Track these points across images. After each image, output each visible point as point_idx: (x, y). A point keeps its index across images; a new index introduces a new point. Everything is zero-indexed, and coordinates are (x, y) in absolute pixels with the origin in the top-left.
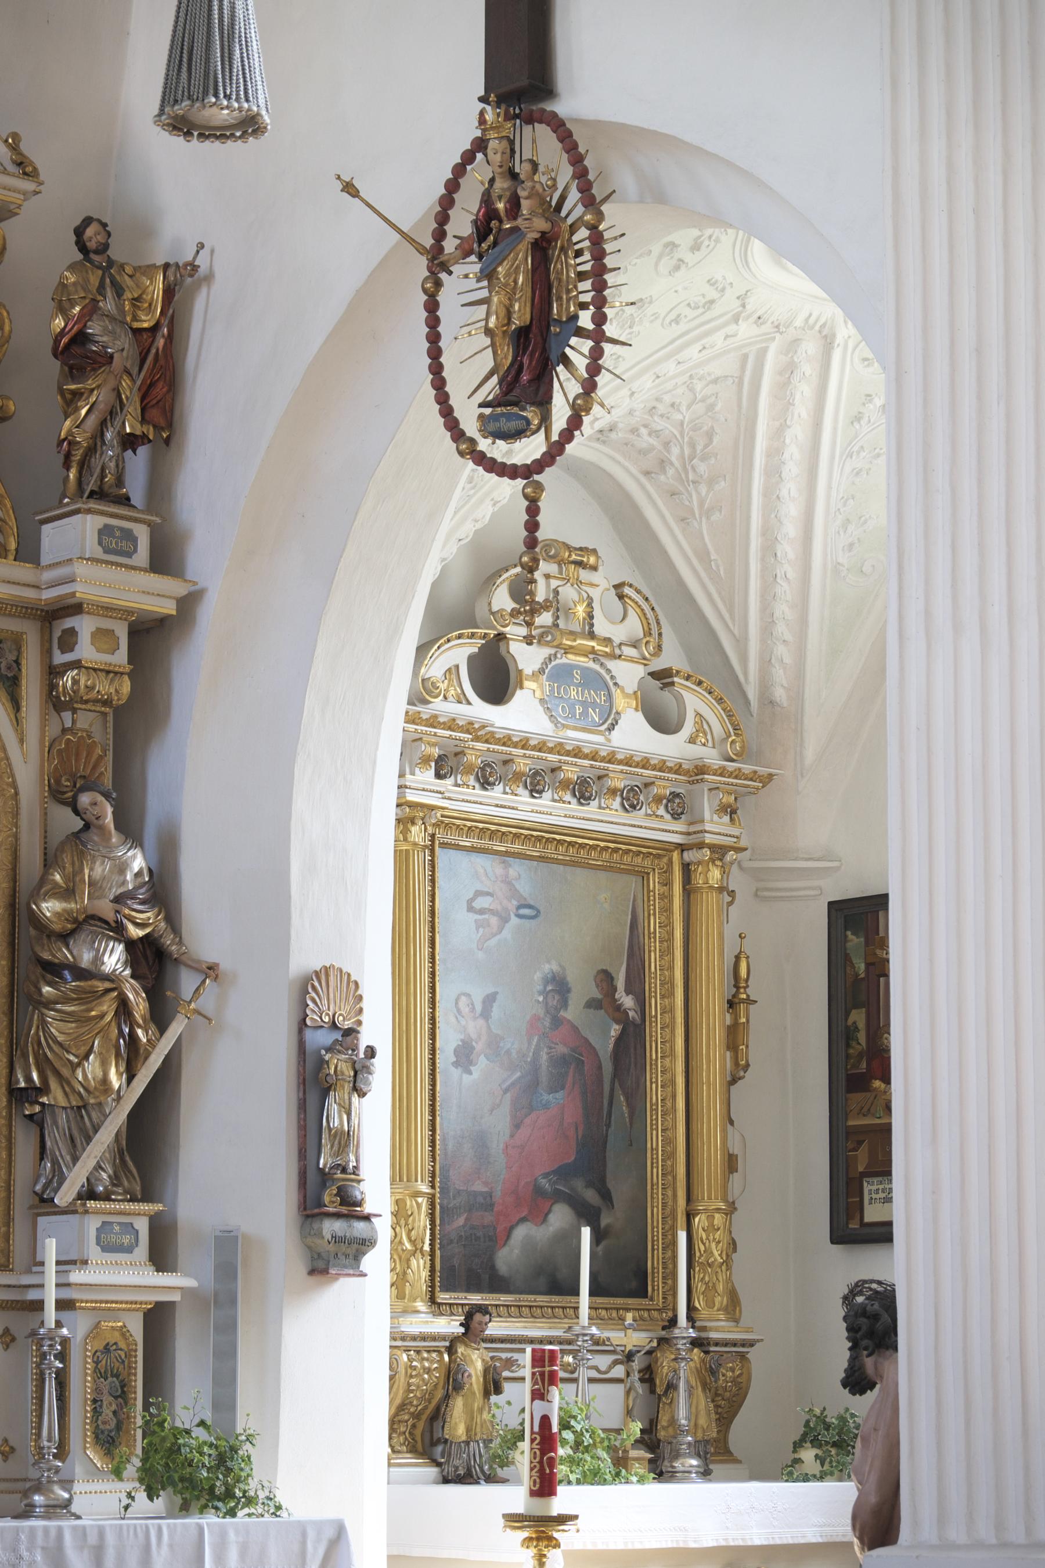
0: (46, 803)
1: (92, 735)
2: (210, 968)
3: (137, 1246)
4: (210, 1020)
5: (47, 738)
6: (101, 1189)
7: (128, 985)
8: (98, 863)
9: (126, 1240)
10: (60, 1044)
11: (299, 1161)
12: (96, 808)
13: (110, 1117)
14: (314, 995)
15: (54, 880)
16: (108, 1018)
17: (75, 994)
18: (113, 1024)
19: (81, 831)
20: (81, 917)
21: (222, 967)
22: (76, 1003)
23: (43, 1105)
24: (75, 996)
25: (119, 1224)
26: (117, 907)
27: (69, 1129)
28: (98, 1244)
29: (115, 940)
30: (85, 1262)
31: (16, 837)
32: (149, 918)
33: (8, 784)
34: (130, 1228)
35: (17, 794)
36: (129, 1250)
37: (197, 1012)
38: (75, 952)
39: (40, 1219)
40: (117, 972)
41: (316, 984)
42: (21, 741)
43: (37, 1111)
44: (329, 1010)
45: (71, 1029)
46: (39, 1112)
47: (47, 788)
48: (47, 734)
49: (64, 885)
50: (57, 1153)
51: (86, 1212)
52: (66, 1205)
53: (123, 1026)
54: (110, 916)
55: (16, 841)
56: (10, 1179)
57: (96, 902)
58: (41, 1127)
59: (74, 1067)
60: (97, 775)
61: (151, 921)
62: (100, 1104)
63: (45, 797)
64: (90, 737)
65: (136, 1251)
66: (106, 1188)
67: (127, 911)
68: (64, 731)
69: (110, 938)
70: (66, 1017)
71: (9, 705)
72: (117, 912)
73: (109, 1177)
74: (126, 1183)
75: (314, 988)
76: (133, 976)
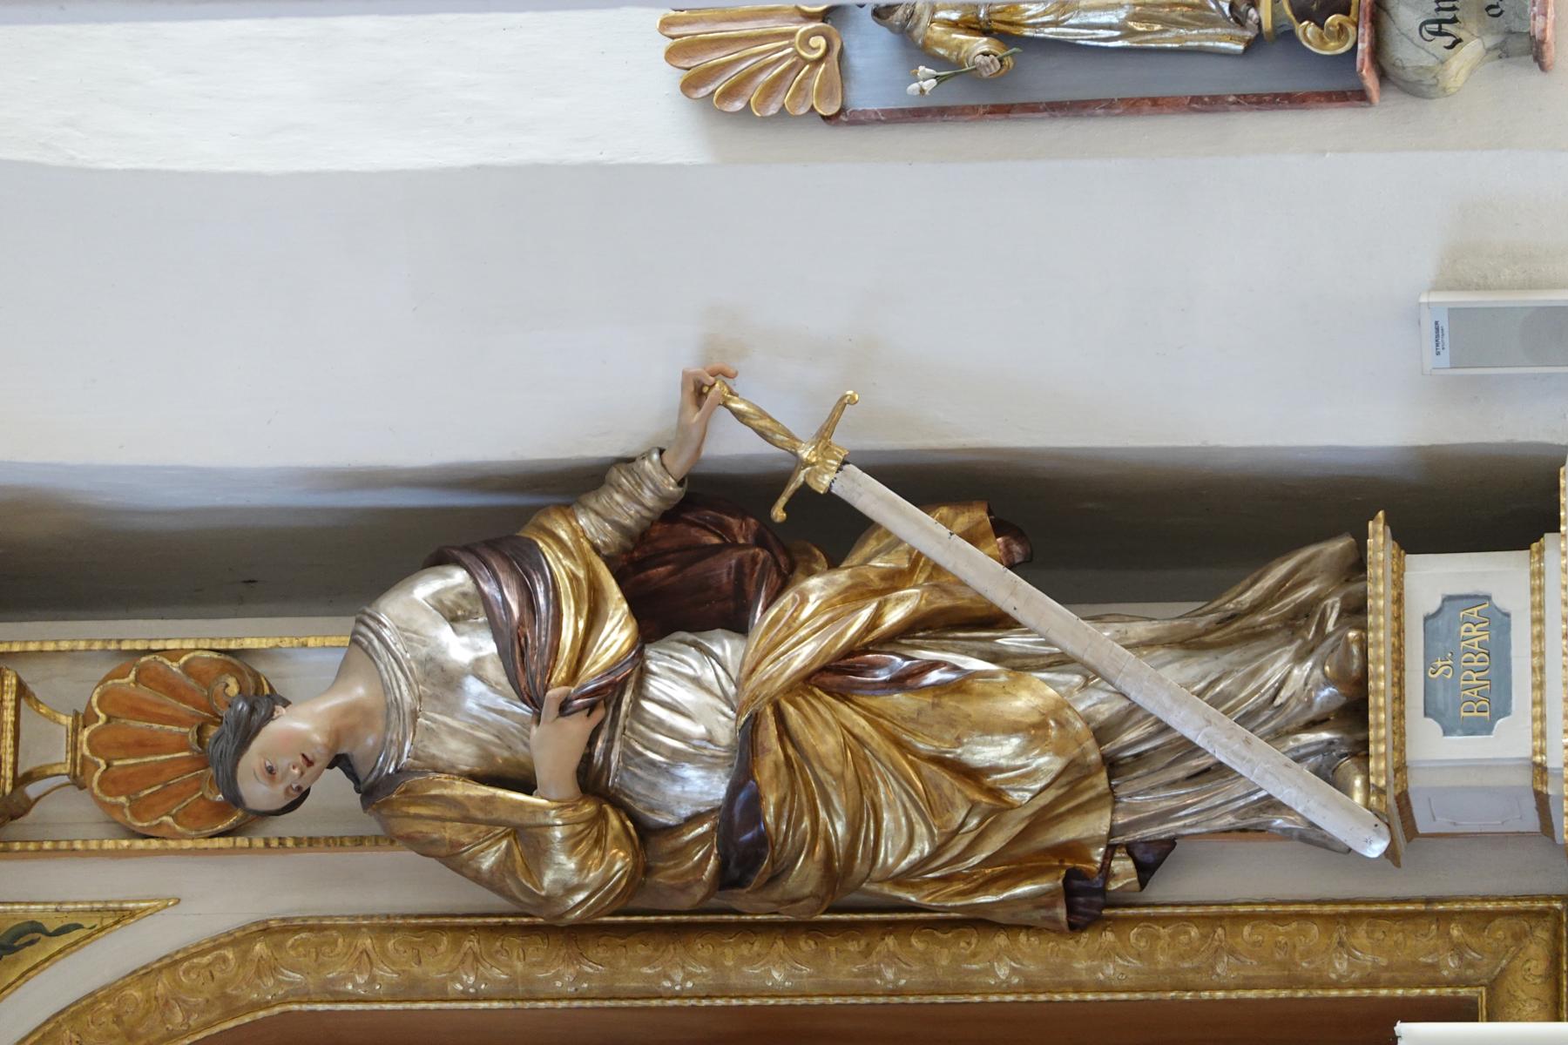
0: (281, 840)
1: (82, 710)
2: (699, 392)
3: (1488, 598)
4: (843, 403)
5: (109, 844)
6: (1326, 692)
7: (768, 669)
8: (434, 750)
9: (1475, 635)
10: (936, 852)
11: (1226, 110)
12: (282, 763)
13: (1133, 695)
14: (754, 92)
15: (491, 870)
16: (861, 724)
17: (799, 820)
18: (875, 702)
19: (351, 774)
20: (589, 809)
21: (695, 367)
22: (823, 814)
23: (1109, 857)
24: (806, 823)
25: (1428, 660)
26: (550, 708)
27: (1173, 784)
28: (1486, 728)
29: (640, 691)
30: (1540, 770)
31: (386, 927)
32: (573, 578)
33: (243, 959)
34: (1440, 622)
35: (265, 930)
36: (1500, 622)
37: (824, 436)
38: (686, 811)
39: (1422, 827)
40: (732, 690)
41: (718, 85)
42: (123, 916)
43: (1129, 864)
44: (792, 34)
45: (897, 821)
46: (1131, 854)
47: (241, 841)
48: (93, 845)
49: (504, 844)
50: (1241, 803)
51: (1401, 768)
52: (1384, 829)
53: (883, 675)
54: (577, 727)
55: (394, 929)
56: (1321, 916)
57: (541, 777)
58: (1170, 844)
59: (999, 804)
60: (191, 682)
61: (581, 574)
62: (1102, 733)
63: (267, 844)
64: (86, 718)
65: (1500, 601)
66: (1328, 681)
67: (561, 673)
68: (78, 781)
69: (636, 708)
70: (864, 813)
71: (30, 956)
72: (564, 708)
73: (1300, 658)
74: (1309, 590)
75: (730, 93)
76: (738, 625)
